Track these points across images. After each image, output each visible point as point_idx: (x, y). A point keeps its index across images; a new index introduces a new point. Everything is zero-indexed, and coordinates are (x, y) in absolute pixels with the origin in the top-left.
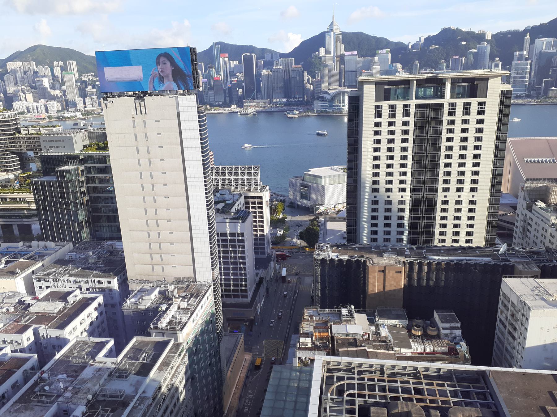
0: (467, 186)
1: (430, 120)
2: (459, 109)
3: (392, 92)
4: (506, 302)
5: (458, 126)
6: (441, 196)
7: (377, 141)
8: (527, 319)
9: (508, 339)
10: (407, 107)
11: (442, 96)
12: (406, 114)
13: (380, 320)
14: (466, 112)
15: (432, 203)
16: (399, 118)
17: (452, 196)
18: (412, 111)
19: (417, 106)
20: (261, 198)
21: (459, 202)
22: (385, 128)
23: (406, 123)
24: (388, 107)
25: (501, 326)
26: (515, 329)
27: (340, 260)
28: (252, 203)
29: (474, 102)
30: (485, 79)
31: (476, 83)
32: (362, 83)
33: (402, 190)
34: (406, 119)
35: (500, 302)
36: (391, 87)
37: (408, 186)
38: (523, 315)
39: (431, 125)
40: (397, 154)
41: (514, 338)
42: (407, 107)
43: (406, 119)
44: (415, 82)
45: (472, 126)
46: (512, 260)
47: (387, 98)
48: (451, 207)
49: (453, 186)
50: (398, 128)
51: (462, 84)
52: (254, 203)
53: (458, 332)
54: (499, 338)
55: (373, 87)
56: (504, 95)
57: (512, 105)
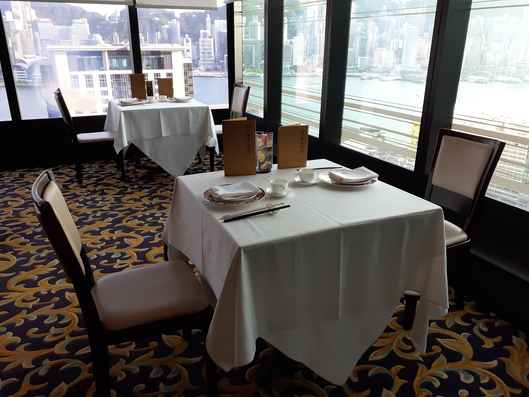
1: (126, 89)
3: (86, 63)
10: (103, 76)
12: (103, 84)
18: (109, 81)
24: (84, 77)
30: (169, 53)
31: (162, 56)
32: (52, 52)
39: (128, 94)
42: (103, 76)
43: (104, 89)
44: (106, 53)
47: (82, 68)
51: (150, 57)
55: (65, 57)
56: (186, 67)
57: (194, 77)
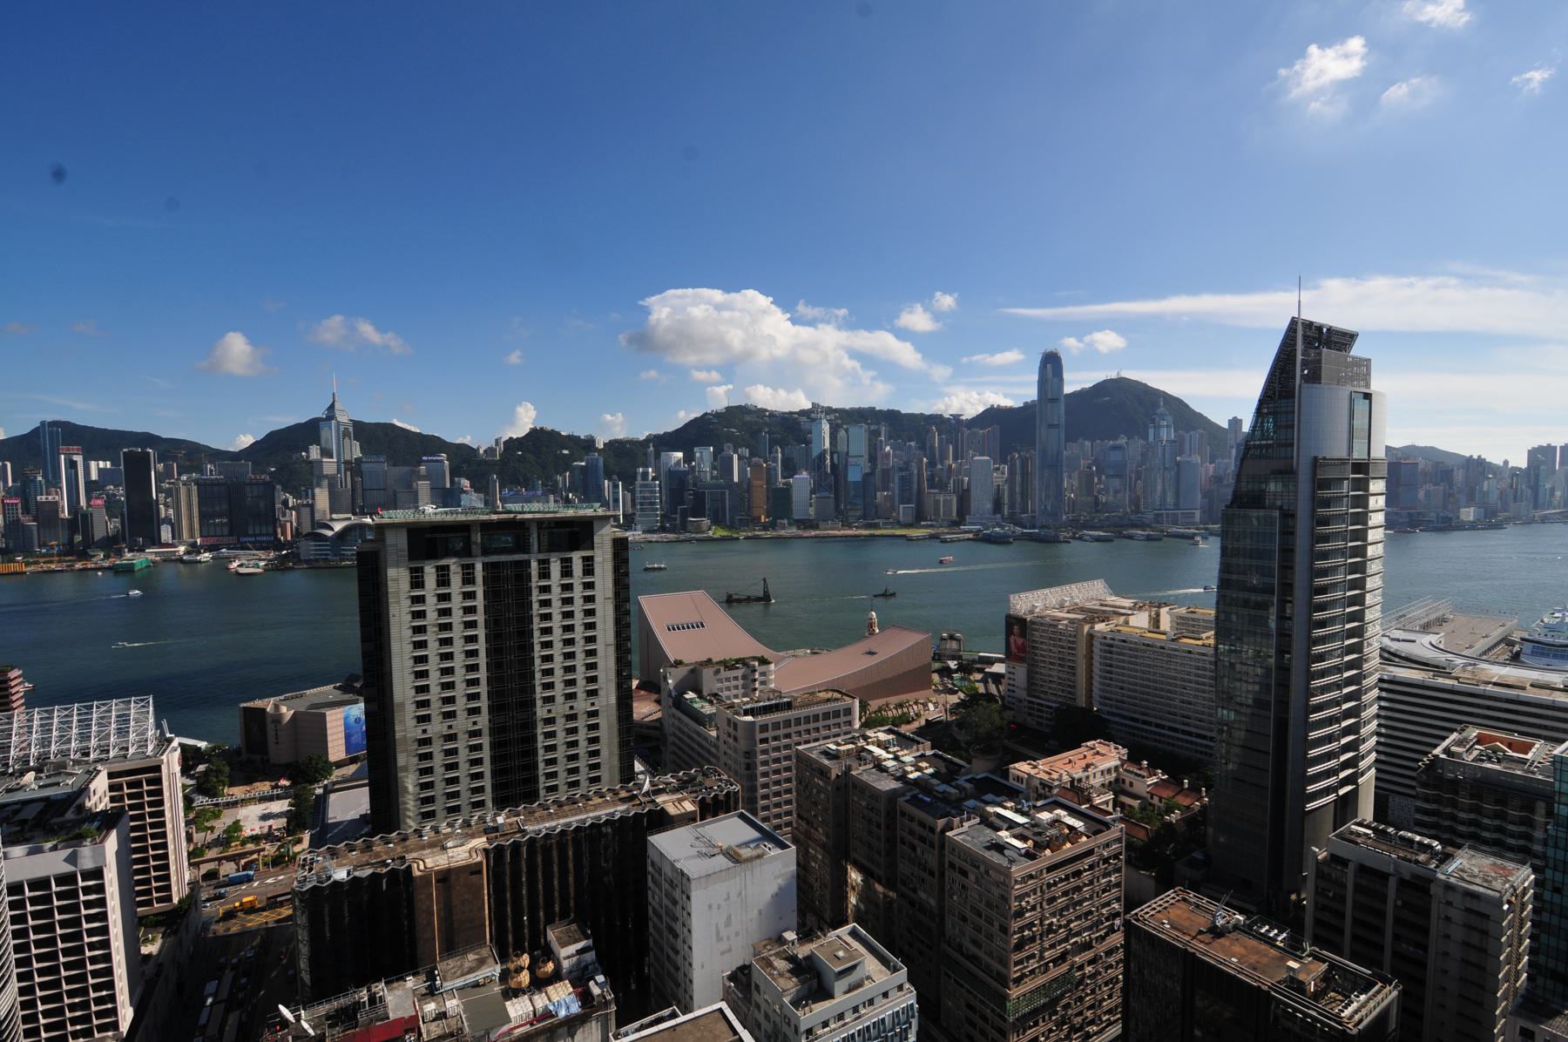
0: (581, 688)
2: (555, 568)
4: (657, 876)
5: (556, 595)
6: (541, 712)
7: (420, 630)
8: (688, 898)
9: (668, 938)
11: (526, 549)
12: (468, 579)
13: (444, 985)
14: (567, 572)
15: (530, 725)
16: (456, 586)
17: (560, 708)
19: (485, 566)
20: (158, 769)
21: (572, 717)
22: (431, 605)
23: (470, 596)
24: (434, 570)
25: (655, 919)
26: (676, 919)
27: (355, 877)
28: (130, 785)
29: (577, 557)
33: (475, 711)
34: (469, 589)
35: (650, 877)
36: (437, 535)
37: (483, 703)
38: (683, 892)
40: (458, 648)
41: (676, 936)
43: (469, 589)
45: (578, 593)
46: (660, 799)
47: (432, 555)
48: (560, 727)
49: (559, 690)
50: (456, 603)
52: (138, 784)
54: (655, 941)
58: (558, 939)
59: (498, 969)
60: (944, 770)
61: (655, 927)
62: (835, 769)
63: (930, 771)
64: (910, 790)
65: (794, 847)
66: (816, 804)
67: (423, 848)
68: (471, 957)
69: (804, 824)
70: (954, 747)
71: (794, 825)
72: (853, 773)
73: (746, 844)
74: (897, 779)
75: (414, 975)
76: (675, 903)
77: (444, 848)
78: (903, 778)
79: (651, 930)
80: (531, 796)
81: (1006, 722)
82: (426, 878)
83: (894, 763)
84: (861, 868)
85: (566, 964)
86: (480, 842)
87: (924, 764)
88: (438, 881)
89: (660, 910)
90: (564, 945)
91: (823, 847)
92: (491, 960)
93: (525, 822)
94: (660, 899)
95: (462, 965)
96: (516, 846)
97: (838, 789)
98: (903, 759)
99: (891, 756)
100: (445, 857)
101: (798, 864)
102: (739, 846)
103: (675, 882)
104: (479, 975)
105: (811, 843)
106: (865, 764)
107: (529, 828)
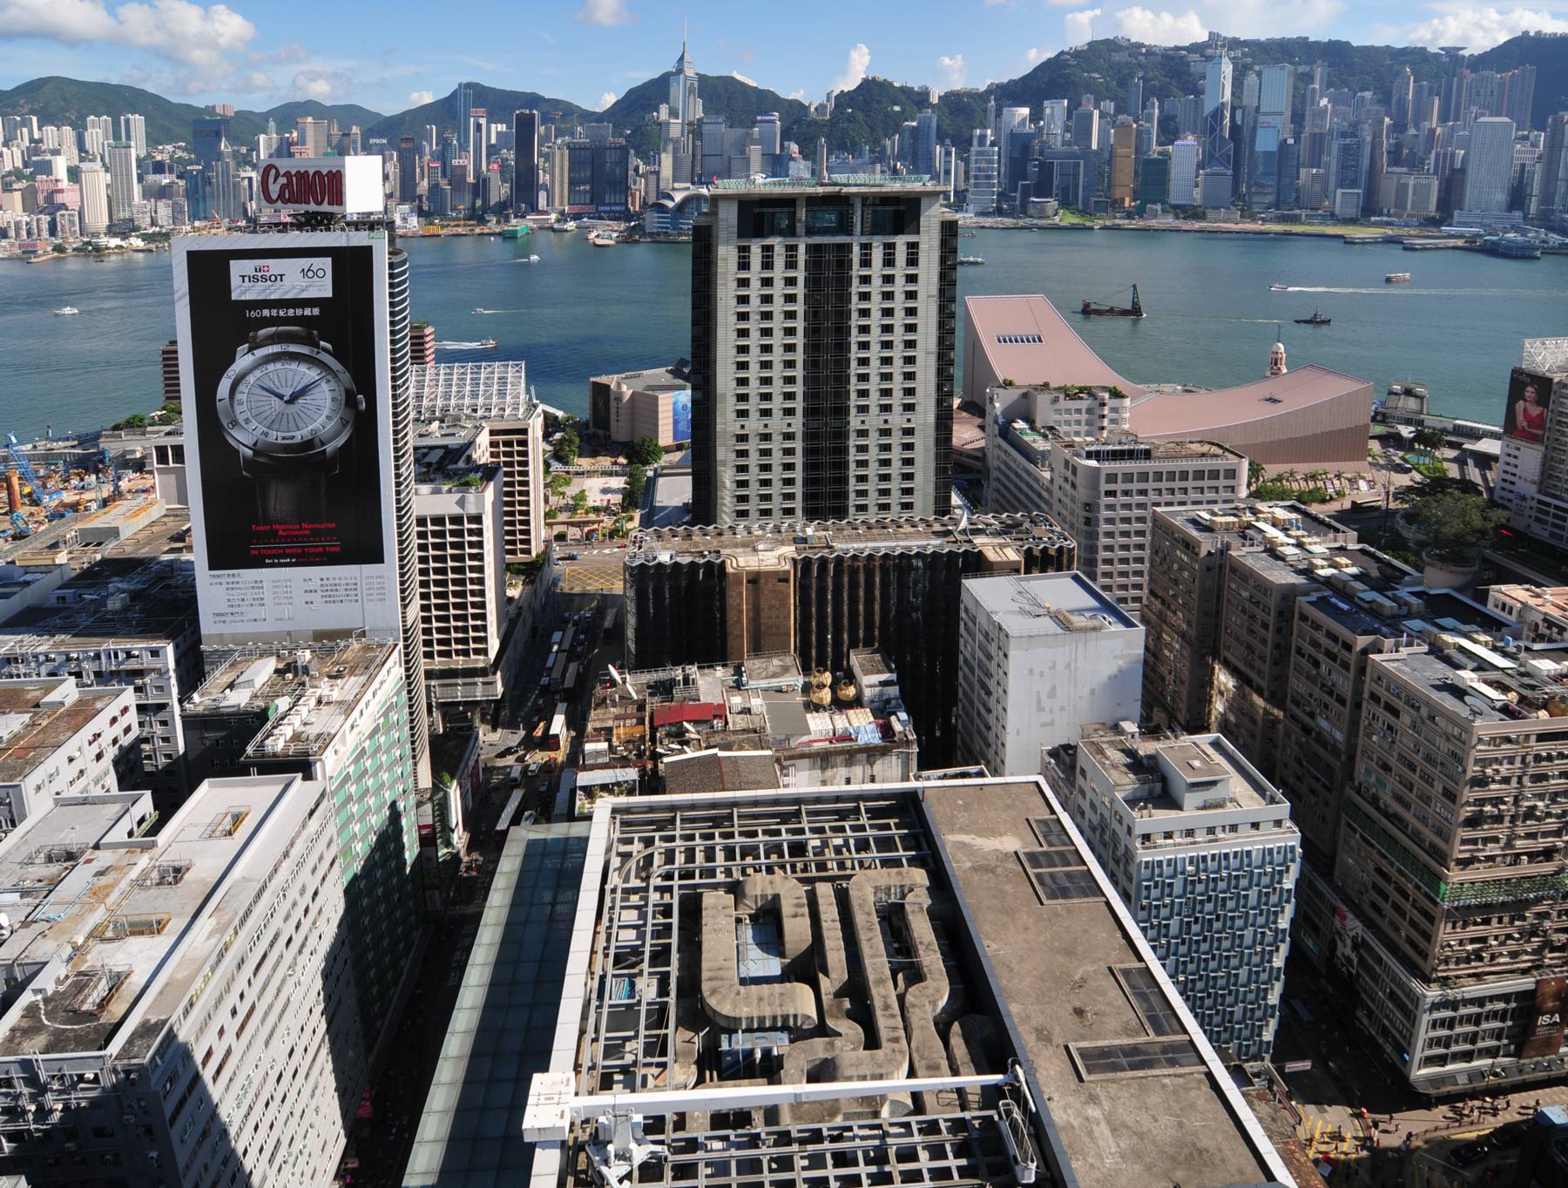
25: (966, 670)
35: (962, 624)
37: (799, 404)
53: (894, 691)
58: (861, 666)
59: (800, 680)
60: (1375, 573)
61: (965, 677)
62: (1207, 544)
63: (1354, 570)
64: (1318, 590)
65: (1142, 628)
66: (1176, 582)
67: (736, 546)
68: (776, 662)
69: (1157, 604)
70: (1397, 545)
71: (1145, 601)
72: (1234, 553)
73: (1080, 611)
74: (1299, 572)
75: (724, 666)
76: (990, 658)
77: (755, 550)
78: (1308, 572)
79: (961, 679)
80: (840, 512)
81: (1490, 525)
82: (738, 576)
83: (1296, 551)
84: (1234, 671)
85: (868, 693)
86: (789, 550)
87: (1343, 560)
88: (749, 581)
89: (972, 661)
90: (867, 673)
91: (1183, 635)
92: (794, 670)
93: (834, 538)
94: (973, 650)
95: (767, 668)
96: (823, 562)
97: (1209, 569)
98: (1308, 547)
99: (1292, 541)
100: (756, 558)
101: (1147, 648)
102: (1071, 612)
103: (991, 635)
104: (783, 681)
105: (1165, 627)
106: (1252, 545)
107: (838, 545)
